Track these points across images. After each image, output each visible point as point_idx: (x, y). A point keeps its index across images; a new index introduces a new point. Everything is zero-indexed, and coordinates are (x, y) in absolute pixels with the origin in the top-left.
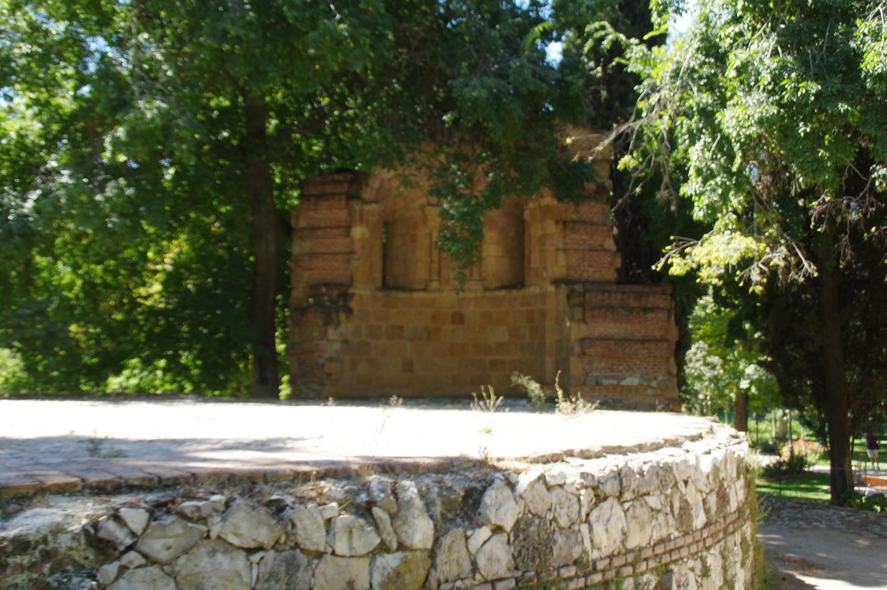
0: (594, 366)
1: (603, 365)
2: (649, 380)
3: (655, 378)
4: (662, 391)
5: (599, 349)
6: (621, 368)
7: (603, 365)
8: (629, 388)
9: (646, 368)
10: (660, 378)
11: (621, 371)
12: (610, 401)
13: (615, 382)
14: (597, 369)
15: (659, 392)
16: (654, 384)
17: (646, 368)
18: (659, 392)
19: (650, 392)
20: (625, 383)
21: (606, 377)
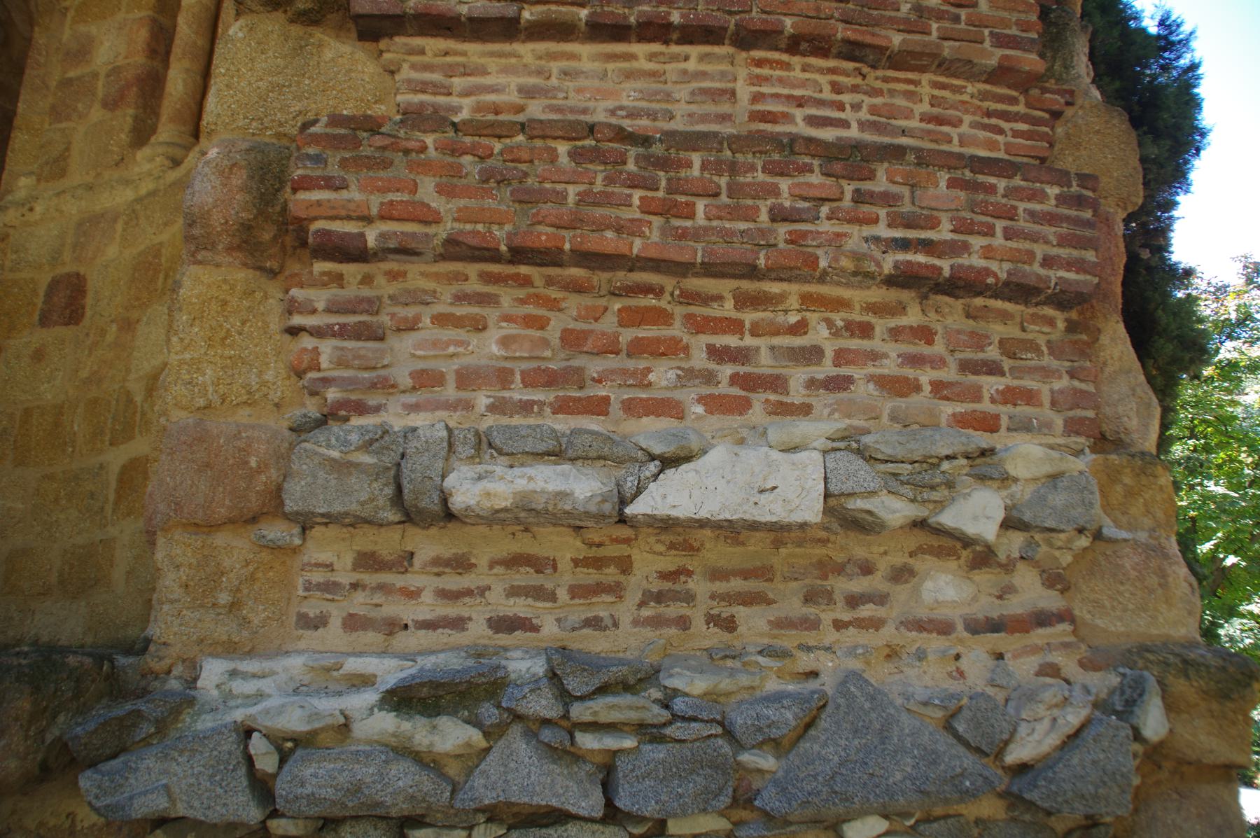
0: (403, 355)
1: (488, 348)
2: (925, 477)
3: (984, 465)
4: (1055, 580)
5: (427, 190)
6: (663, 374)
7: (488, 348)
8: (747, 550)
9: (898, 387)
10: (1027, 456)
11: (667, 408)
12: (524, 665)
13: (583, 486)
14: (426, 379)
15: (1031, 592)
16: (978, 513)
17: (898, 387)
18: (1031, 592)
19: (945, 588)
20: (671, 496)
21: (484, 445)
